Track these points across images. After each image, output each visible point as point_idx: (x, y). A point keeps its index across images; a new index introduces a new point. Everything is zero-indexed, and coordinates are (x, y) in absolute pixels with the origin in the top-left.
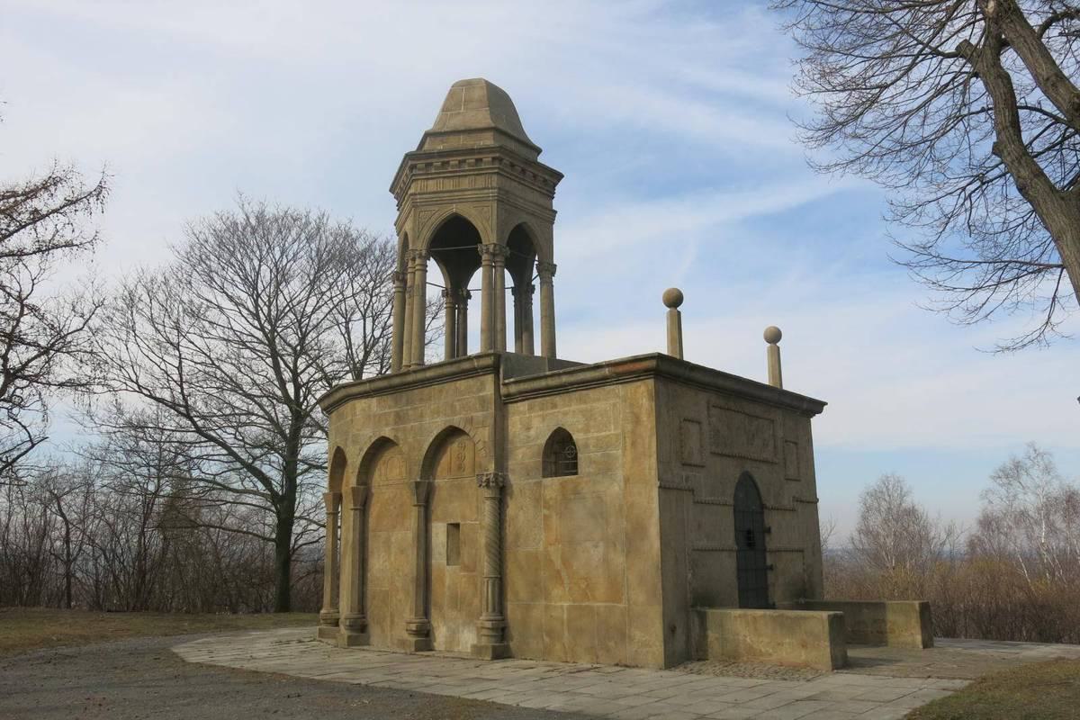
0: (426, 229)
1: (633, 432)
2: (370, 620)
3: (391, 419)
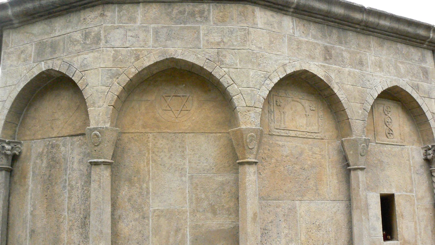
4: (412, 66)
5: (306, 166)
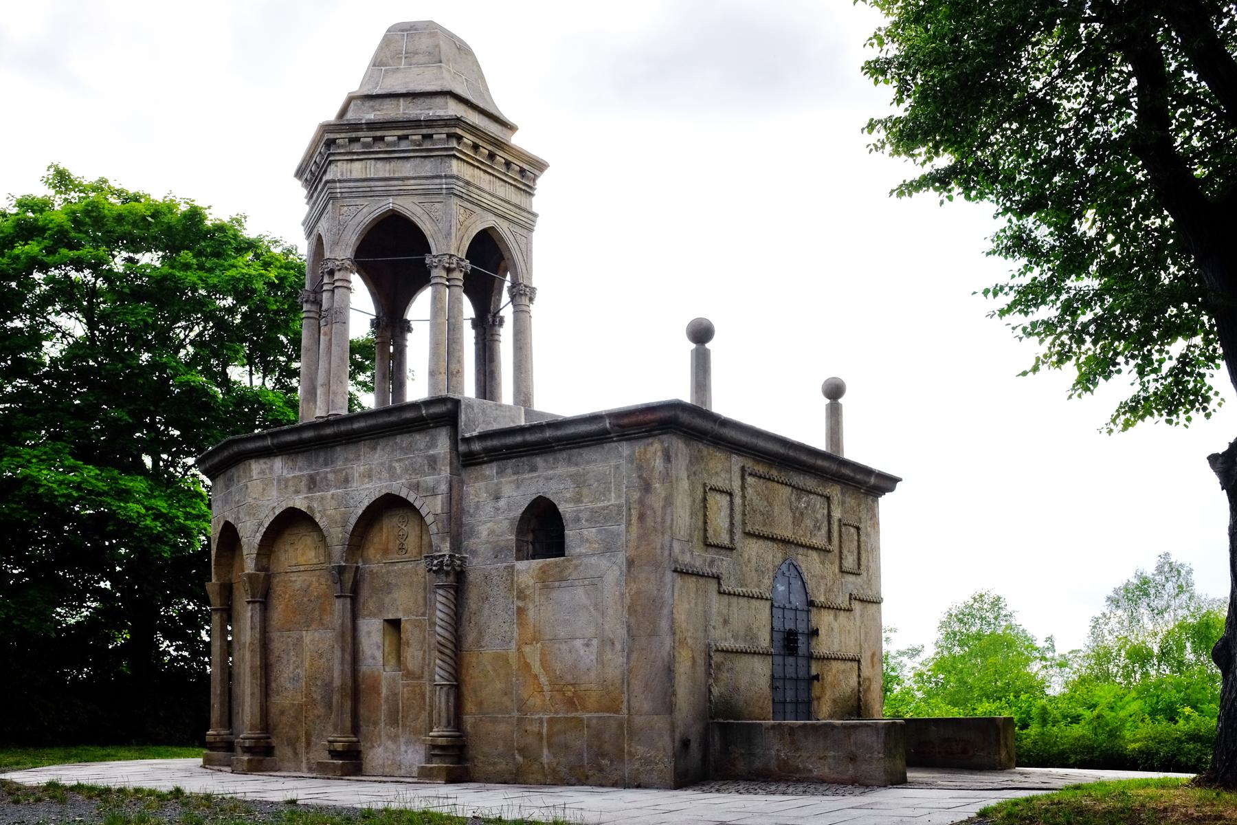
0: (349, 230)
1: (641, 502)
2: (274, 741)
3: (303, 485)
4: (414, 460)
5: (312, 598)
